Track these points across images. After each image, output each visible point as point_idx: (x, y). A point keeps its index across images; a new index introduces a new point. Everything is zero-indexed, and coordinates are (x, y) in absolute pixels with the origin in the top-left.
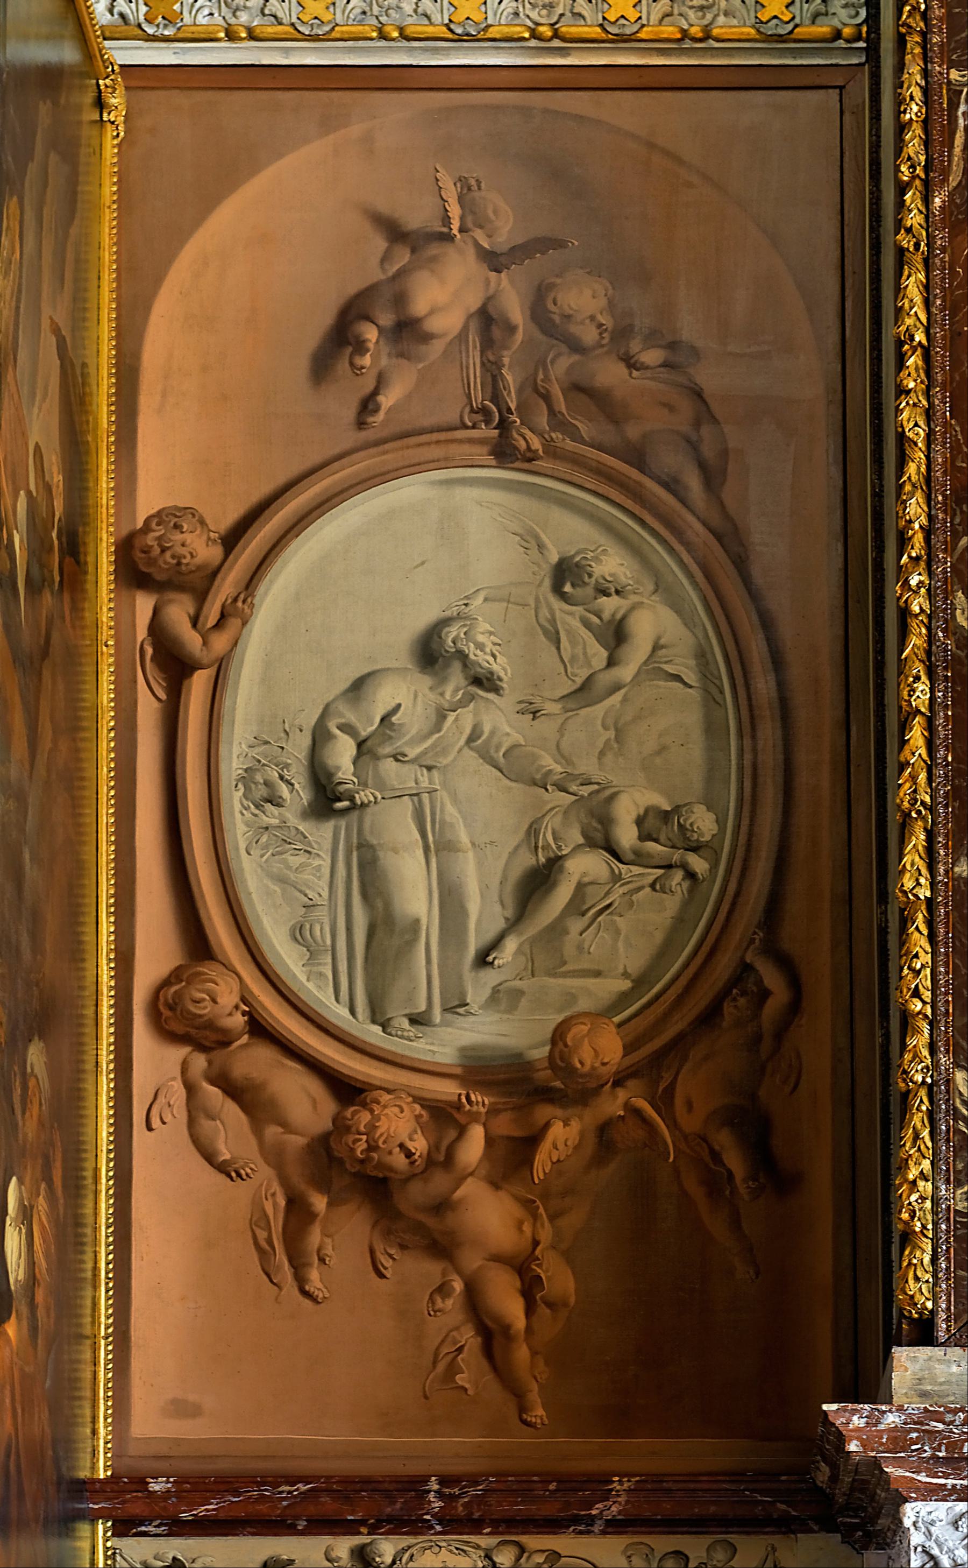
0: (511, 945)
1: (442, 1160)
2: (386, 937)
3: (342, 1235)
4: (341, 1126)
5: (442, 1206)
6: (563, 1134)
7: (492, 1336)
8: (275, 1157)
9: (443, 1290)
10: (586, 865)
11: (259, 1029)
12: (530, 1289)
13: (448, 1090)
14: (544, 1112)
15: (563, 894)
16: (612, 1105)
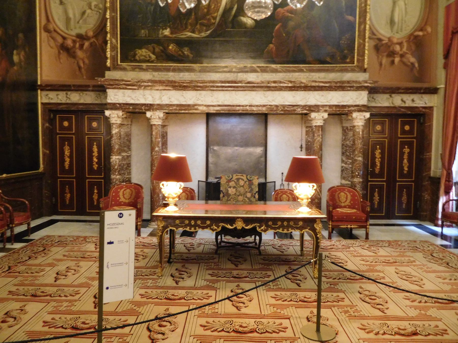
0: (81, 21)
1: (74, 47)
2: (68, 20)
3: (64, 56)
4: (64, 43)
5: (74, 52)
6: (87, 44)
7: (80, 68)
8: (57, 46)
9: (74, 62)
10: (88, 11)
11: (55, 31)
12: (84, 62)
13: (74, 38)
14: (85, 41)
15: (86, 15)
16: (92, 40)
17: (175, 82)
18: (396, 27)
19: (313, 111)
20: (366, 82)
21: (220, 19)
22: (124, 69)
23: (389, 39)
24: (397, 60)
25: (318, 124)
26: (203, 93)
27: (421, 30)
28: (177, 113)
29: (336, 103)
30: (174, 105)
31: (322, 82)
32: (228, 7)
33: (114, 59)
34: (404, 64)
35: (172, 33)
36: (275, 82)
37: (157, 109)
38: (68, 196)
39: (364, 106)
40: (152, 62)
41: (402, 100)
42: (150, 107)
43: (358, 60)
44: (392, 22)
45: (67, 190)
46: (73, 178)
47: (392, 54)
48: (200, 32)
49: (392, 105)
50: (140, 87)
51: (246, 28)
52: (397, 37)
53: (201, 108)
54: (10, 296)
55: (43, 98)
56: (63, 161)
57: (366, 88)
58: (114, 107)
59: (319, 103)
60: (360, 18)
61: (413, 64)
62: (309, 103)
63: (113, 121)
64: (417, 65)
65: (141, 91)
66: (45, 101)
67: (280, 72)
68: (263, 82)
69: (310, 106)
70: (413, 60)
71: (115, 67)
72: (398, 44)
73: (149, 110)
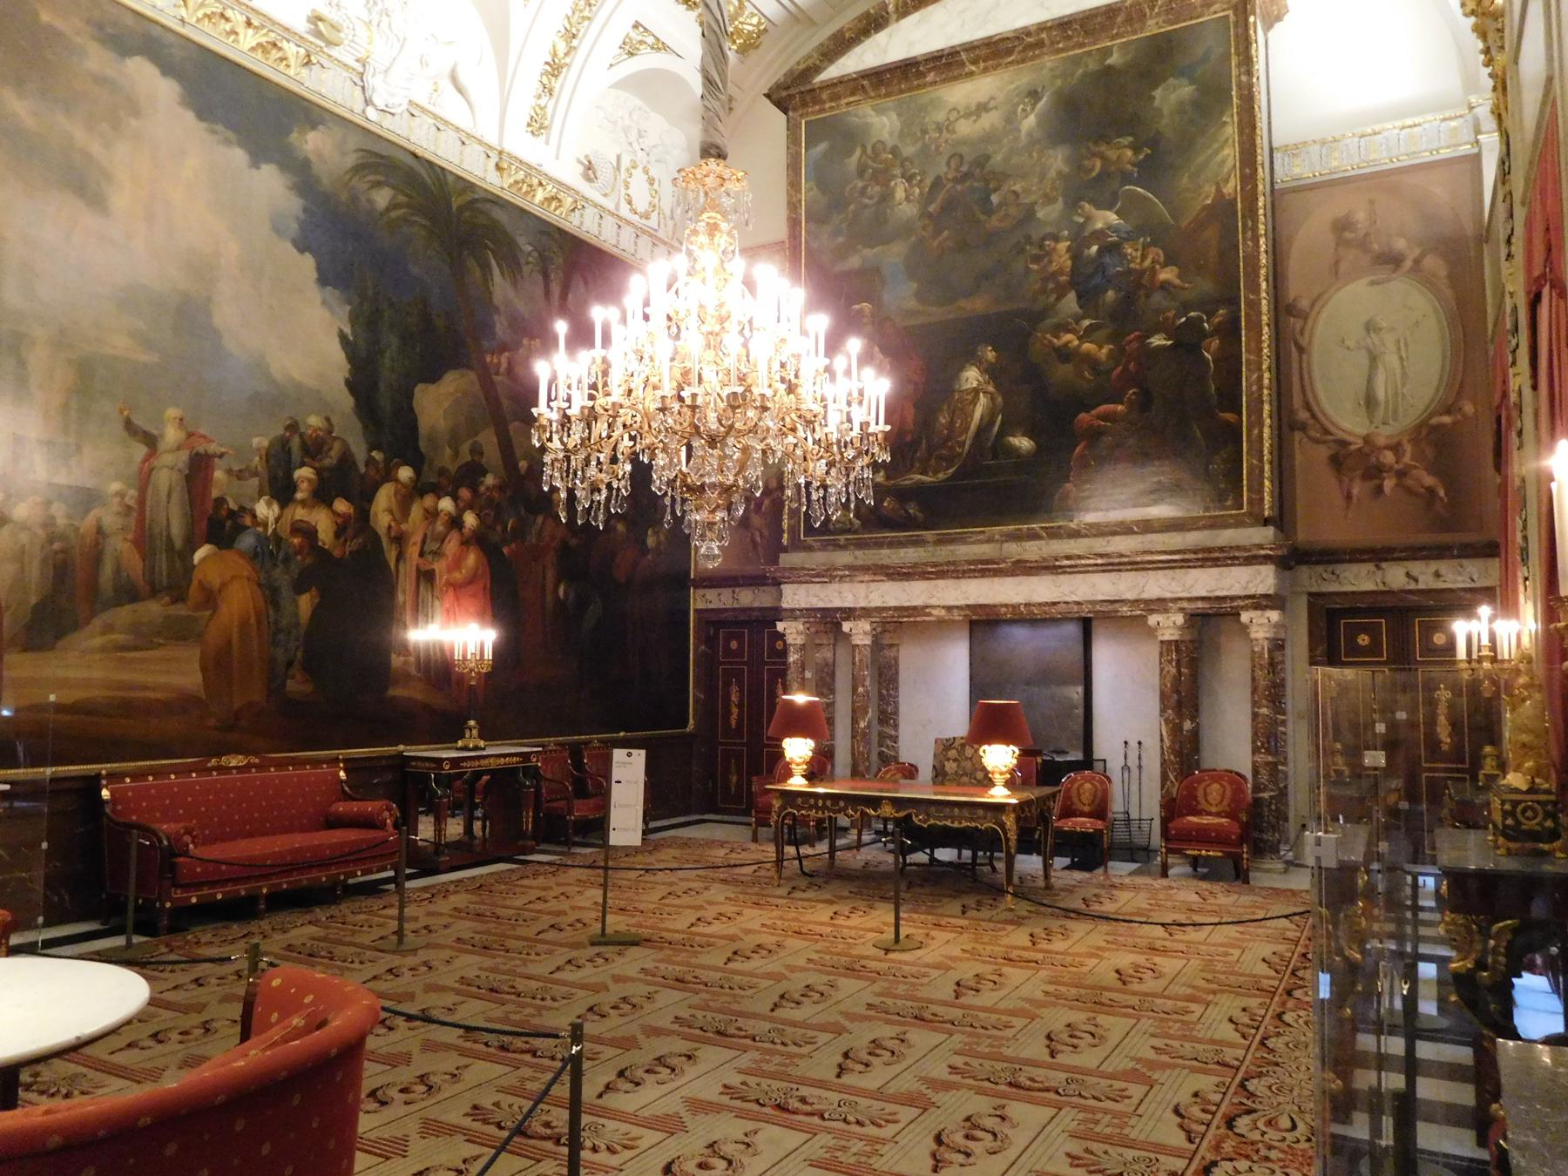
17: (888, 567)
18: (1380, 412)
19: (1153, 611)
20: (1261, 547)
21: (972, 445)
22: (809, 549)
23: (1367, 439)
24: (1389, 484)
25: (1166, 638)
26: (941, 583)
27: (1448, 412)
28: (896, 625)
29: (1204, 594)
30: (889, 609)
31: (1165, 553)
32: (985, 421)
33: (793, 531)
34: (1410, 491)
35: (888, 478)
36: (1068, 558)
37: (860, 617)
38: (735, 779)
39: (1266, 596)
40: (856, 532)
41: (1408, 575)
42: (850, 613)
43: (1250, 502)
44: (1370, 402)
45: (733, 768)
46: (742, 744)
47: (1374, 473)
48: (936, 472)
49: (1382, 588)
50: (832, 579)
51: (1019, 456)
52: (1384, 435)
53: (934, 612)
54: (676, 1027)
55: (701, 600)
56: (728, 713)
57: (1266, 559)
58: (793, 614)
59: (1168, 595)
60: (1249, 416)
61: (1431, 491)
62: (1145, 596)
63: (790, 640)
64: (1442, 493)
65: (835, 586)
66: (701, 606)
67: (1086, 536)
68: (1044, 560)
69: (1147, 602)
70: (1429, 480)
71: (796, 545)
72: (1388, 447)
73: (847, 619)
